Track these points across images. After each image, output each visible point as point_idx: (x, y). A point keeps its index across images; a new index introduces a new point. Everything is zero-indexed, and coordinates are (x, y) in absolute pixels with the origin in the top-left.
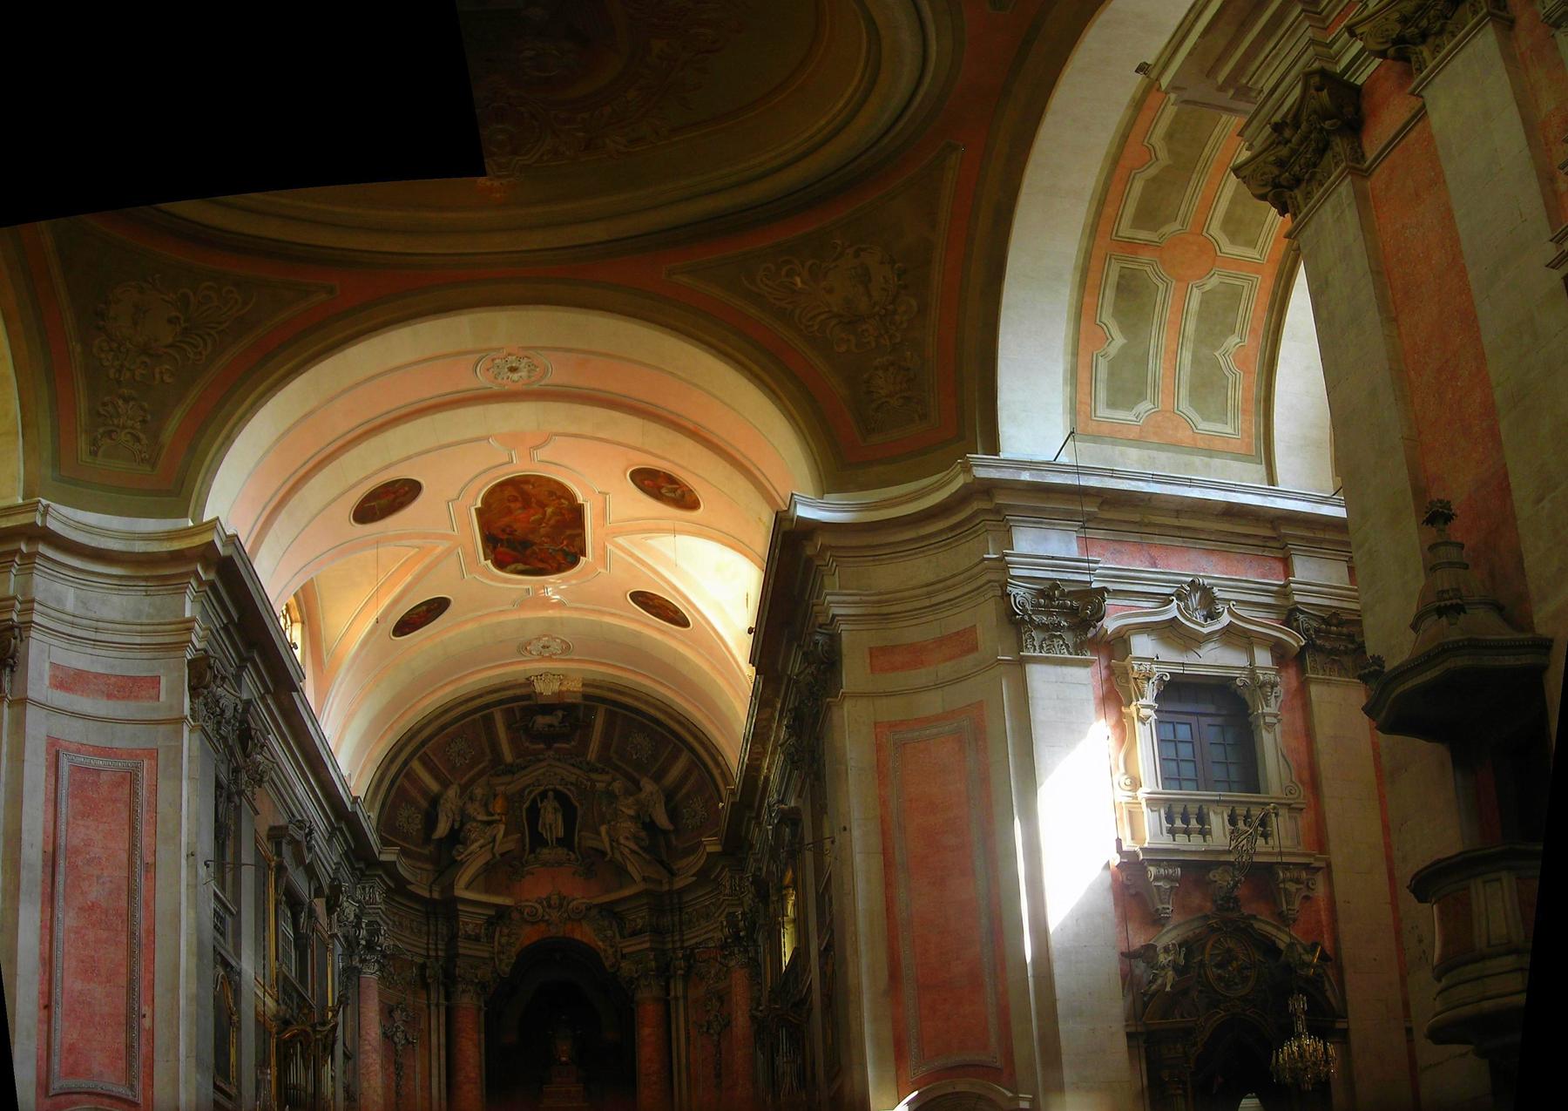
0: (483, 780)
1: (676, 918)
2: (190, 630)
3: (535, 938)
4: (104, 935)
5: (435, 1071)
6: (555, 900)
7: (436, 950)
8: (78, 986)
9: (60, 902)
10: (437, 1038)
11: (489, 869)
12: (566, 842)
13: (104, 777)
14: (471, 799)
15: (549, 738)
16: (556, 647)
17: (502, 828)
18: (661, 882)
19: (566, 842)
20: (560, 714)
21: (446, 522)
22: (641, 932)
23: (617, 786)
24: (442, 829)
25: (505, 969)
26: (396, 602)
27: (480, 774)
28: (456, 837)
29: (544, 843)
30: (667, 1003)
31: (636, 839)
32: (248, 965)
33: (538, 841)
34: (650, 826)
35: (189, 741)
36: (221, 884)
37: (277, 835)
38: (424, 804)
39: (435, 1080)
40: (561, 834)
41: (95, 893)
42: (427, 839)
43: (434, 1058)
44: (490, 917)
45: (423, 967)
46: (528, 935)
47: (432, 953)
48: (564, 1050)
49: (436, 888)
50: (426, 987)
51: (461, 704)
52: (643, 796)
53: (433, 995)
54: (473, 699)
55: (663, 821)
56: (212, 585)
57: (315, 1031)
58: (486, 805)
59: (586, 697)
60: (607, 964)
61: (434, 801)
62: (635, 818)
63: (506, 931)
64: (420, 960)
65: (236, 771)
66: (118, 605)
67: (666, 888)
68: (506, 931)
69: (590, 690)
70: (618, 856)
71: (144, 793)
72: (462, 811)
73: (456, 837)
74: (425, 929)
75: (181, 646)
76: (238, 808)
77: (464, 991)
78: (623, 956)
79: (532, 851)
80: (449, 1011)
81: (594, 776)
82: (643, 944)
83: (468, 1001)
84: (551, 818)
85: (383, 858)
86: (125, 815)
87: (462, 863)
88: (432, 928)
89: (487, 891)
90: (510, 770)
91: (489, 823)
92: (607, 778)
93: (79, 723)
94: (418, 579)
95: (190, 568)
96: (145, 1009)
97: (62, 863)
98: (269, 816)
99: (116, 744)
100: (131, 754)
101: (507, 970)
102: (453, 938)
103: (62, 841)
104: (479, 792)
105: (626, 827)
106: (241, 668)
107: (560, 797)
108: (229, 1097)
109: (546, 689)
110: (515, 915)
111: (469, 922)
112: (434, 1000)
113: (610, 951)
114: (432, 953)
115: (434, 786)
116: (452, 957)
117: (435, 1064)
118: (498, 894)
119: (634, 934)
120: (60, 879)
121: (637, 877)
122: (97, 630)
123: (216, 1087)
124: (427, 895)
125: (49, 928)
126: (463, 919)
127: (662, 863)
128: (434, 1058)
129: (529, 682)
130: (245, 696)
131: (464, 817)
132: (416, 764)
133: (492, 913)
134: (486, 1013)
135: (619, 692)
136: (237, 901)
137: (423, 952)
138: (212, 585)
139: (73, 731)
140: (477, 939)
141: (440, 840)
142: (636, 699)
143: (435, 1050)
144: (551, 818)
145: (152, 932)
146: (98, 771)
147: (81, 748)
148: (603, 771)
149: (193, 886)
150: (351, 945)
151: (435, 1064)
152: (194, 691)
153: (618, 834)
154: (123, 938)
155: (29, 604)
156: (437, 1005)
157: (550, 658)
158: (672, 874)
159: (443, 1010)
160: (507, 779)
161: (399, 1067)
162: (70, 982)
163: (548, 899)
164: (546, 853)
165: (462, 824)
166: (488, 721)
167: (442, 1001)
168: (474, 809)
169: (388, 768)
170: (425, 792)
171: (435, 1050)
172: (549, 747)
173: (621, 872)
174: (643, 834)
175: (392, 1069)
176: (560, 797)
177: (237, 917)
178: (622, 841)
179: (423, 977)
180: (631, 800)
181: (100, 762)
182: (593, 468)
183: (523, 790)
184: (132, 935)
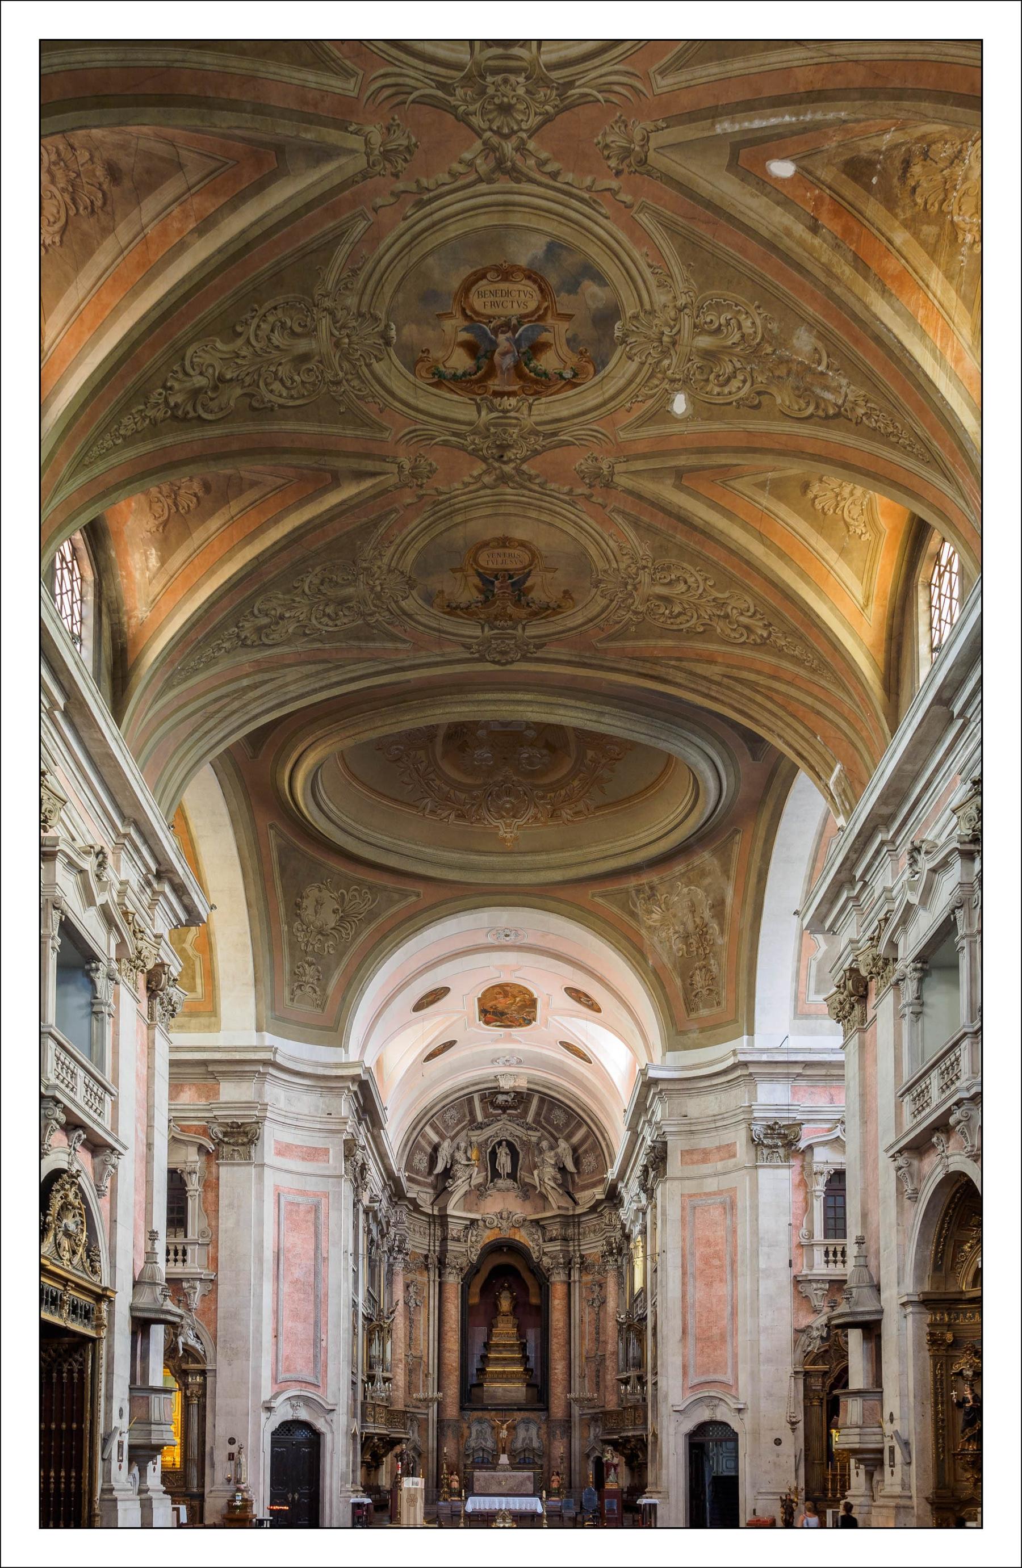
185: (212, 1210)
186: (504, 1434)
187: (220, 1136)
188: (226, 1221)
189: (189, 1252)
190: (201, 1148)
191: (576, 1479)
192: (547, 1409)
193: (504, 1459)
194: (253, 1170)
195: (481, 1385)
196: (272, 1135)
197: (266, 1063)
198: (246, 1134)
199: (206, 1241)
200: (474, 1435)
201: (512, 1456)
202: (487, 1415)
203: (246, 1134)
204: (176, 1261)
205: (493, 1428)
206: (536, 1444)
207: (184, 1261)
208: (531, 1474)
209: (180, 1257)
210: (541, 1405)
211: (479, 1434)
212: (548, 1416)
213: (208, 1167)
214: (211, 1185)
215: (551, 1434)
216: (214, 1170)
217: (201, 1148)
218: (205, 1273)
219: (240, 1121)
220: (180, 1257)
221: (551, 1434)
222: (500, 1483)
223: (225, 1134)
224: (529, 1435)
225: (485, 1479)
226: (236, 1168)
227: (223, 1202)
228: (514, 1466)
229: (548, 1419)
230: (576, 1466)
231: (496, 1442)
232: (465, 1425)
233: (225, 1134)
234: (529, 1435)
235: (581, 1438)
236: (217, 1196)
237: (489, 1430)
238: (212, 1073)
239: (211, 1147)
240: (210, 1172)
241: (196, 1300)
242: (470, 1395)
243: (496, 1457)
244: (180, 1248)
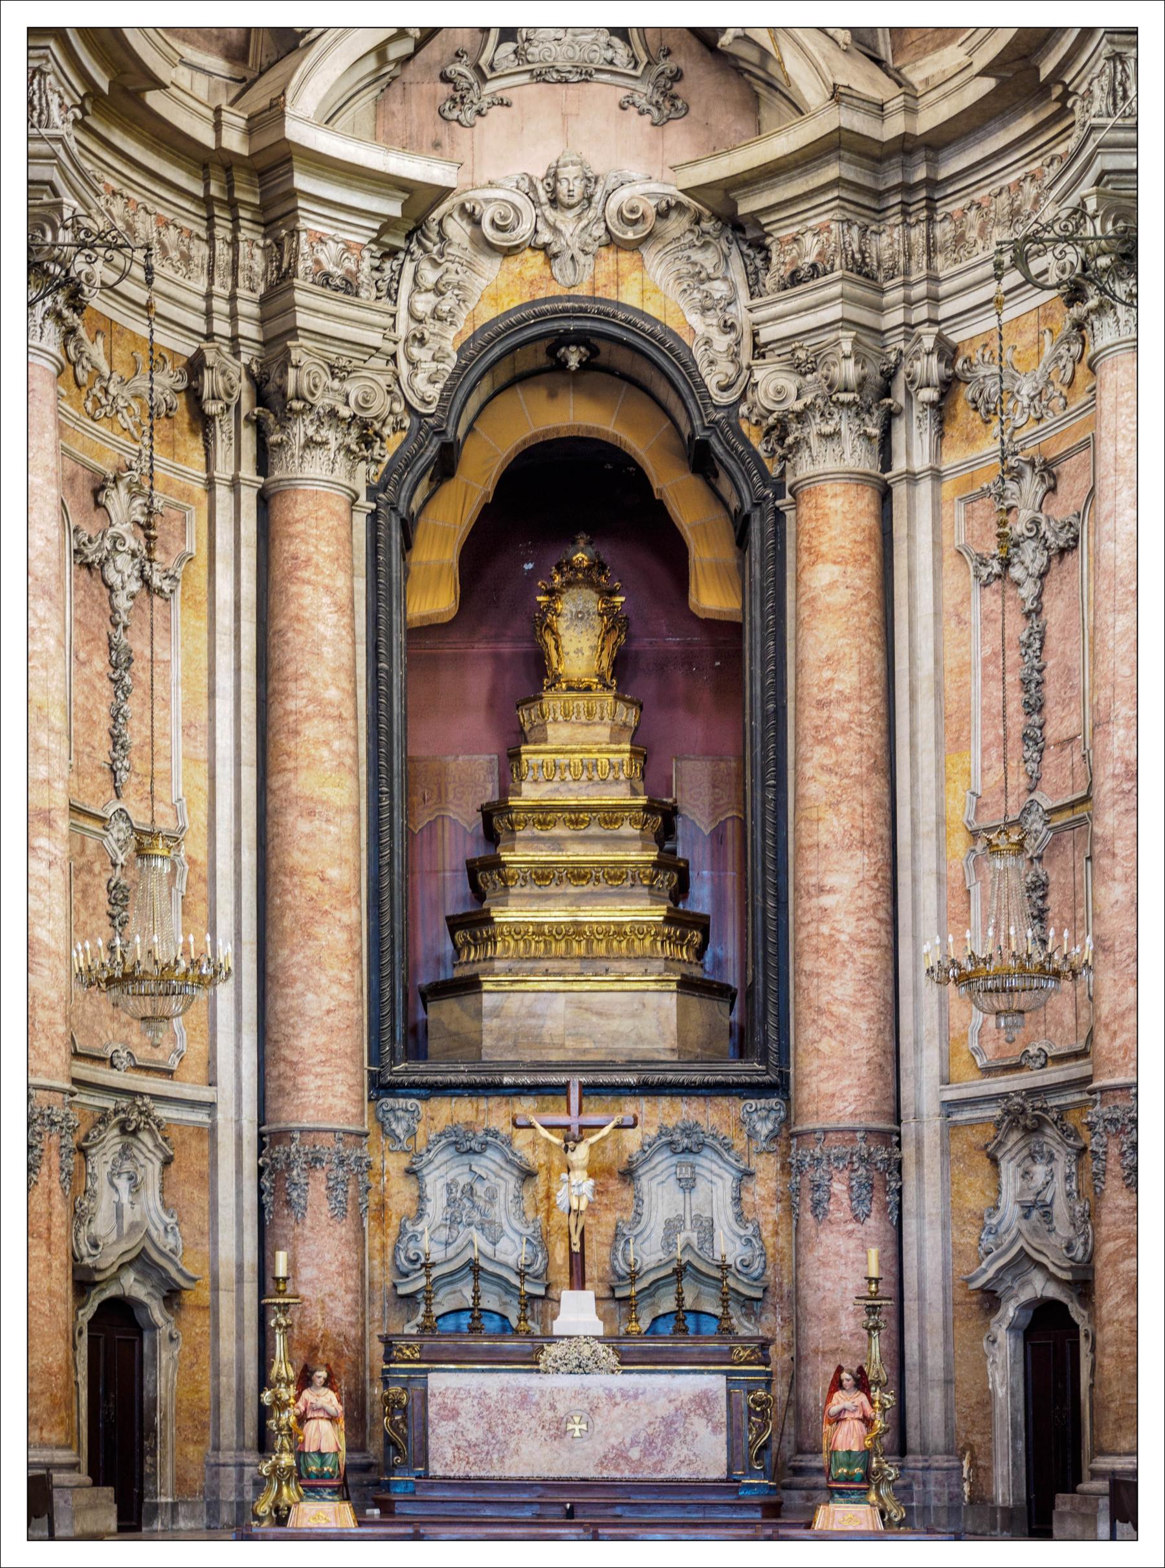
1: (917, 234)
5: (224, 681)
7: (233, 316)
10: (234, 584)
22: (815, 271)
30: (885, 495)
39: (225, 707)
43: (224, 641)
44: (388, 225)
45: (195, 366)
47: (222, 327)
50: (202, 423)
63: (430, 276)
64: (186, 348)
68: (430, 276)
74: (200, 251)
77: (311, 443)
78: (759, 350)
80: (264, 500)
83: (326, 484)
88: (223, 253)
89: (383, 137)
101: (434, 392)
112: (224, 470)
114: (222, 327)
117: (224, 660)
118: (409, 145)
119: (795, 279)
121: (812, 92)
126: (310, 222)
127: (878, 62)
128: (224, 641)
133: (393, 209)
134: (373, 516)
137: (200, 325)
140: (349, 286)
143: (224, 619)
151: (224, 660)
156: (235, 485)
159: (249, 498)
161: (120, 661)
167: (248, 471)
171: (224, 619)
175: (100, 663)
179: (194, 396)
186: (576, 1189)
191: (930, 1410)
192: (779, 1087)
193: (578, 1313)
195: (470, 986)
200: (436, 1207)
201: (619, 1299)
202: (495, 1115)
205: (527, 1175)
206: (728, 1246)
208: (714, 1383)
210: (750, 1069)
211: (466, 1200)
212: (786, 1122)
215: (799, 1201)
221: (799, 1201)
222: (559, 1430)
224: (698, 1203)
225: (486, 1410)
228: (632, 1355)
229: (787, 1134)
230: (928, 1343)
231: (541, 1242)
232: (395, 1164)
234: (698, 1203)
235: (952, 1216)
237: (507, 1184)
242: (417, 1025)
243: (540, 1304)
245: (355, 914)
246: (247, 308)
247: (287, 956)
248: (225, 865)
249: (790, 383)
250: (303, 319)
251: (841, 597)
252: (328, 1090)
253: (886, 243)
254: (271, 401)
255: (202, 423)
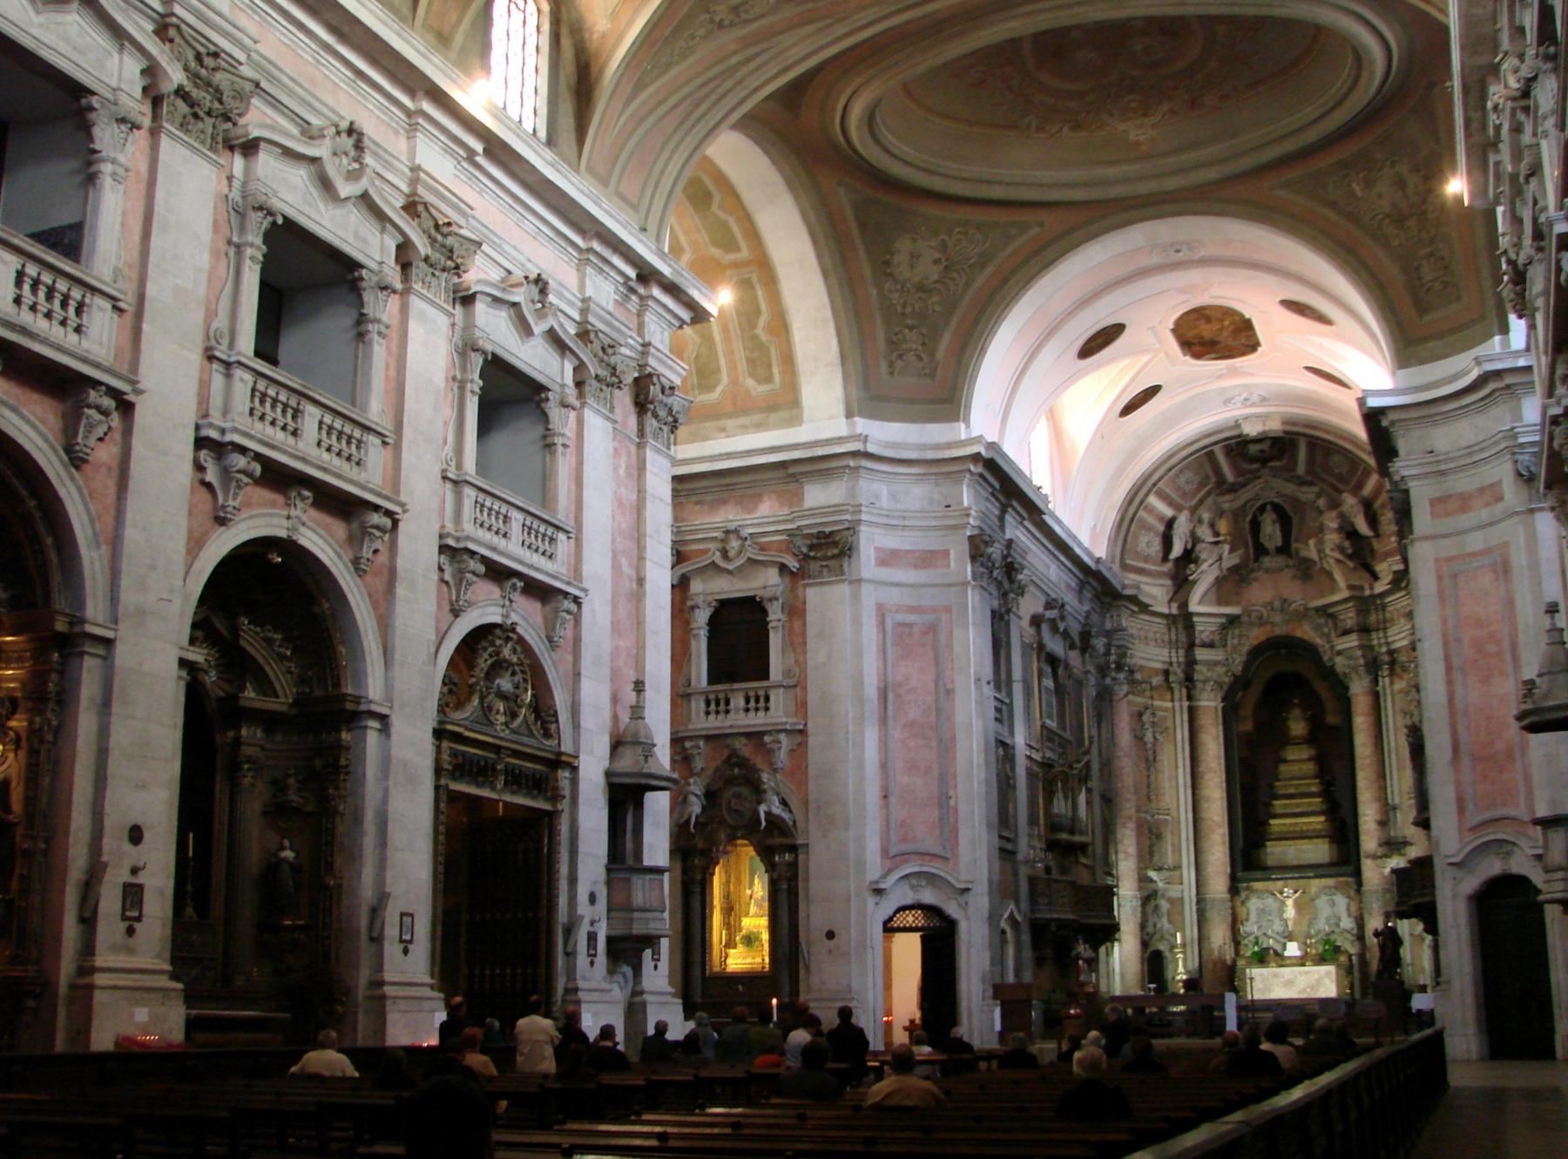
0: (1210, 500)
2: (968, 515)
3: (1263, 638)
4: (921, 742)
6: (1277, 604)
8: (906, 780)
9: (891, 723)
10: (1182, 734)
11: (1219, 581)
12: (1284, 550)
13: (916, 629)
14: (1200, 521)
15: (1263, 459)
16: (1255, 398)
17: (1226, 547)
18: (1361, 588)
19: (1284, 550)
20: (1268, 442)
21: (1149, 353)
23: (1321, 502)
24: (1177, 550)
25: (1238, 669)
26: (1118, 398)
27: (1209, 493)
28: (1189, 557)
29: (1265, 552)
31: (1341, 549)
32: (1020, 739)
33: (1260, 551)
34: (1351, 534)
35: (973, 597)
36: (998, 688)
37: (1036, 621)
38: (1161, 528)
40: (1279, 542)
41: (913, 713)
42: (1165, 559)
45: (1166, 673)
46: (1256, 635)
48: (1298, 727)
49: (1174, 605)
51: (1184, 447)
52: (1345, 508)
53: (1177, 695)
54: (1192, 443)
55: (1363, 527)
56: (981, 475)
57: (1071, 767)
58: (1212, 525)
59: (1286, 432)
60: (1326, 658)
61: (1170, 524)
62: (1340, 529)
65: (1005, 594)
66: (916, 495)
67: (1367, 593)
69: (1288, 428)
70: (1326, 565)
71: (943, 638)
72: (1193, 535)
73: (1189, 557)
75: (964, 526)
76: (1008, 624)
79: (1256, 560)
81: (1305, 489)
82: (1352, 641)
83: (1210, 702)
84: (1271, 532)
85: (1127, 592)
86: (931, 654)
87: (1194, 582)
90: (1233, 489)
91: (1216, 543)
92: (1315, 489)
93: (896, 591)
94: (1133, 379)
95: (965, 467)
96: (951, 793)
97: (891, 696)
98: (1029, 605)
99: (923, 603)
100: (933, 610)
102: (1191, 646)
103: (890, 680)
104: (1206, 516)
105: (1332, 538)
106: (1004, 512)
107: (1277, 509)
108: (1008, 840)
109: (1251, 430)
110: (1245, 619)
111: (1205, 629)
113: (1327, 646)
115: (1169, 512)
116: (1190, 663)
119: (1346, 632)
120: (890, 706)
122: (904, 518)
123: (1001, 837)
124: (1165, 610)
125: (884, 742)
126: (1198, 628)
129: (1237, 425)
130: (1008, 536)
131: (1195, 539)
132: (1153, 500)
133: (1223, 620)
135: (1314, 428)
136: (1010, 694)
138: (981, 475)
139: (893, 597)
140: (1211, 645)
141: (1177, 560)
142: (1327, 432)
144: (1271, 532)
145: (953, 739)
146: (911, 625)
147: (900, 609)
148: (1311, 484)
149: (979, 702)
150: (1103, 671)
151: (1180, 756)
152: (973, 558)
153: (1326, 546)
154: (934, 744)
155: (857, 509)
157: (1252, 405)
158: (1375, 577)
160: (1228, 497)
162: (902, 779)
163: (1271, 603)
164: (1267, 562)
165: (1194, 545)
166: (1210, 456)
168: (1205, 533)
169: (1126, 510)
170: (1161, 518)
171: (1179, 745)
172: (1264, 466)
173: (1329, 574)
174: (1347, 544)
176: (1277, 509)
177: (1010, 706)
178: (1328, 551)
179: (1167, 680)
180: (1334, 514)
181: (911, 618)
182: (1255, 300)
183: (1244, 506)
184: (940, 741)
185: (796, 642)
187: (805, 550)
188: (816, 655)
189: (772, 698)
190: (783, 568)
194: (844, 589)
196: (870, 542)
197: (855, 454)
198: (836, 544)
199: (792, 682)
203: (836, 544)
204: (757, 709)
207: (767, 709)
209: (762, 704)
213: (793, 589)
214: (796, 611)
216: (800, 592)
217: (783, 568)
218: (791, 721)
219: (828, 530)
220: (762, 704)
223: (811, 547)
226: (826, 588)
227: (811, 632)
233: (811, 547)
236: (805, 625)
238: (793, 475)
239: (793, 564)
240: (796, 597)
241: (782, 757)
244: (761, 693)
245: (1225, 830)
246: (1181, 652)
247: (1205, 844)
248: (1183, 818)
249: (1346, 662)
250: (1198, 657)
251: (1364, 726)
252: (1218, 884)
253: (1373, 618)
254: (1189, 679)
255: (1171, 689)
